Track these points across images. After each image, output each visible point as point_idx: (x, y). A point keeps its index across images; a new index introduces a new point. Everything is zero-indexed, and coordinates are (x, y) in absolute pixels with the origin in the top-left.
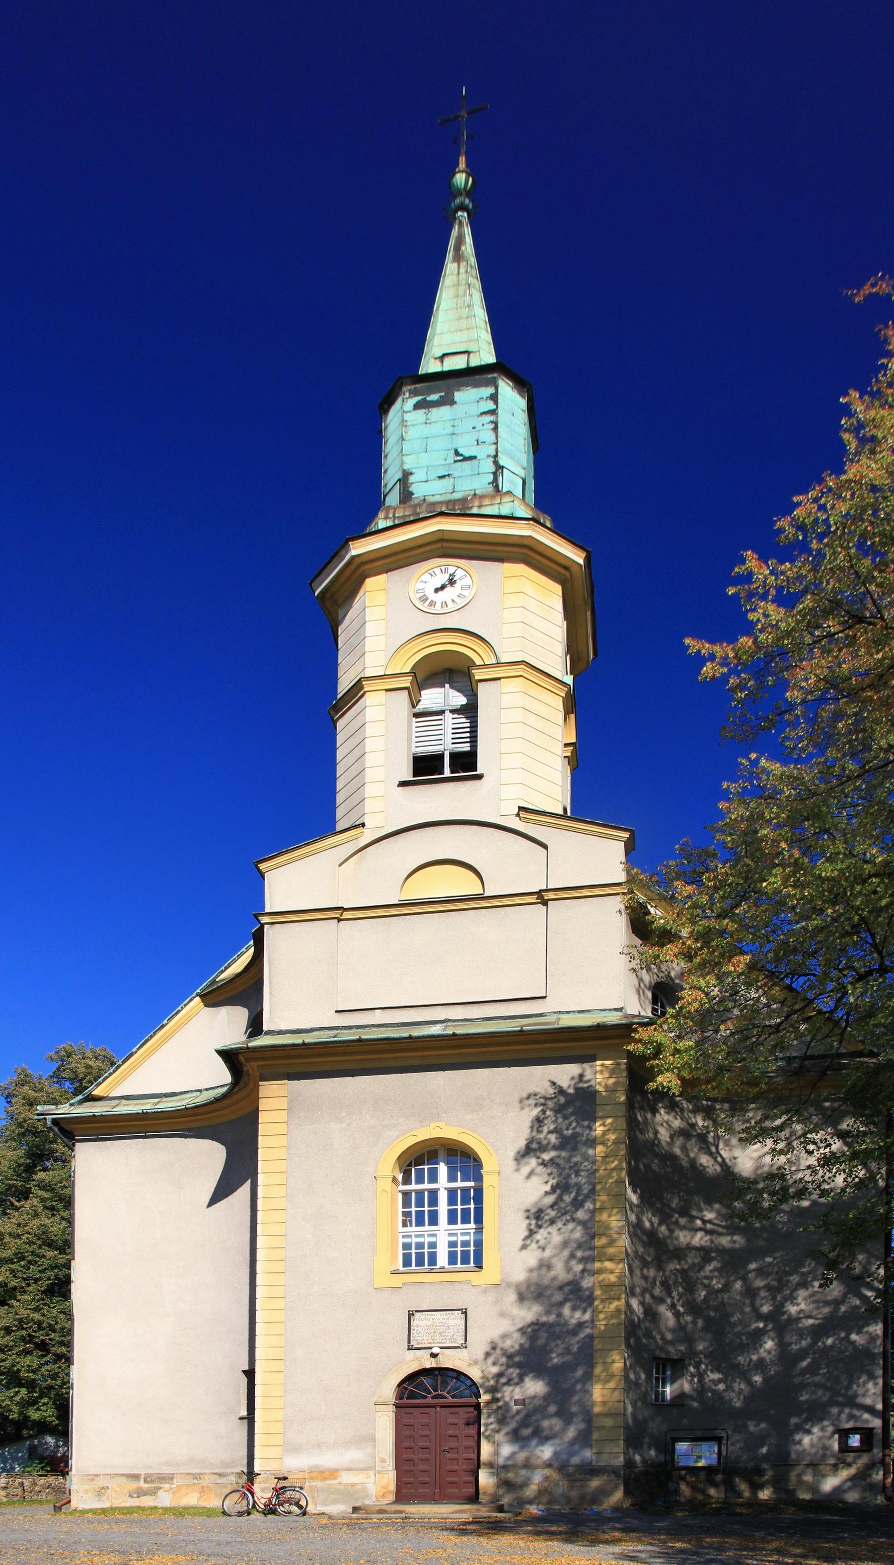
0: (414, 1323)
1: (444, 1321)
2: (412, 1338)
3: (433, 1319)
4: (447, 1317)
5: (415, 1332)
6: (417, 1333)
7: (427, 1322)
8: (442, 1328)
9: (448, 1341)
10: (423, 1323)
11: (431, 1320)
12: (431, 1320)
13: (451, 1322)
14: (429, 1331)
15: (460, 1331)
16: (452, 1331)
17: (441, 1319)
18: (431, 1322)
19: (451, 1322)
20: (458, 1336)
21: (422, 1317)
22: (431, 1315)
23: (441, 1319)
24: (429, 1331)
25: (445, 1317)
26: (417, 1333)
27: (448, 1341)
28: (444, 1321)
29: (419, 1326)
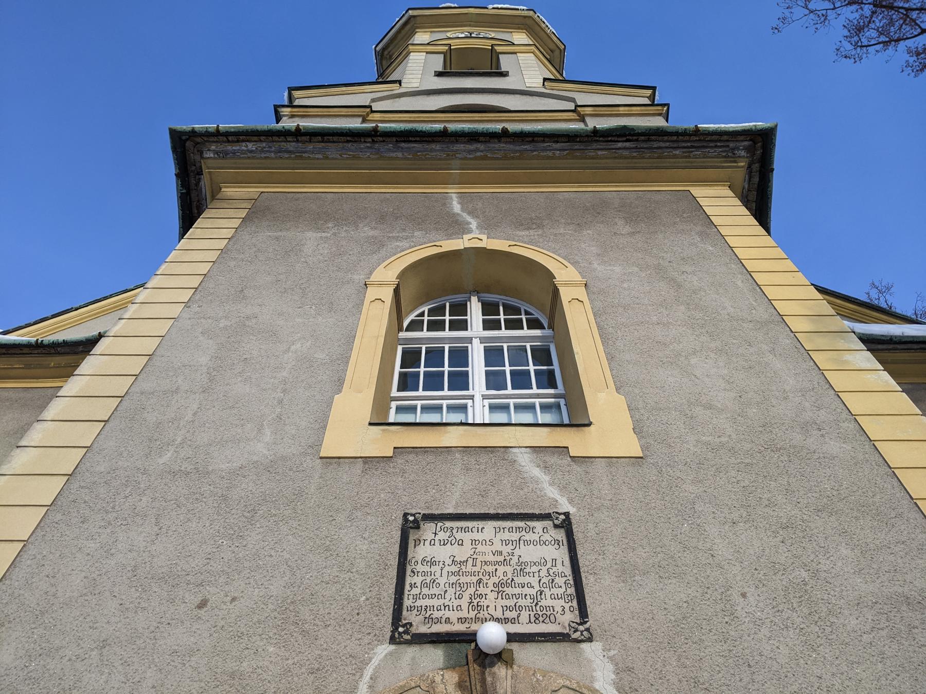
0: (419, 553)
1: (506, 549)
2: (407, 602)
3: (474, 542)
4: (515, 536)
5: (418, 580)
6: (424, 584)
7: (455, 550)
8: (501, 569)
9: (524, 616)
10: (443, 553)
11: (467, 543)
12: (467, 543)
13: (529, 553)
14: (464, 579)
15: (560, 581)
16: (534, 581)
17: (497, 541)
18: (463, 553)
19: (529, 553)
20: (554, 597)
21: (442, 535)
22: (466, 530)
23: (497, 541)
24: (464, 579)
25: (506, 536)
26: (424, 584)
27: (524, 616)
28: (506, 549)
29: (432, 563)
